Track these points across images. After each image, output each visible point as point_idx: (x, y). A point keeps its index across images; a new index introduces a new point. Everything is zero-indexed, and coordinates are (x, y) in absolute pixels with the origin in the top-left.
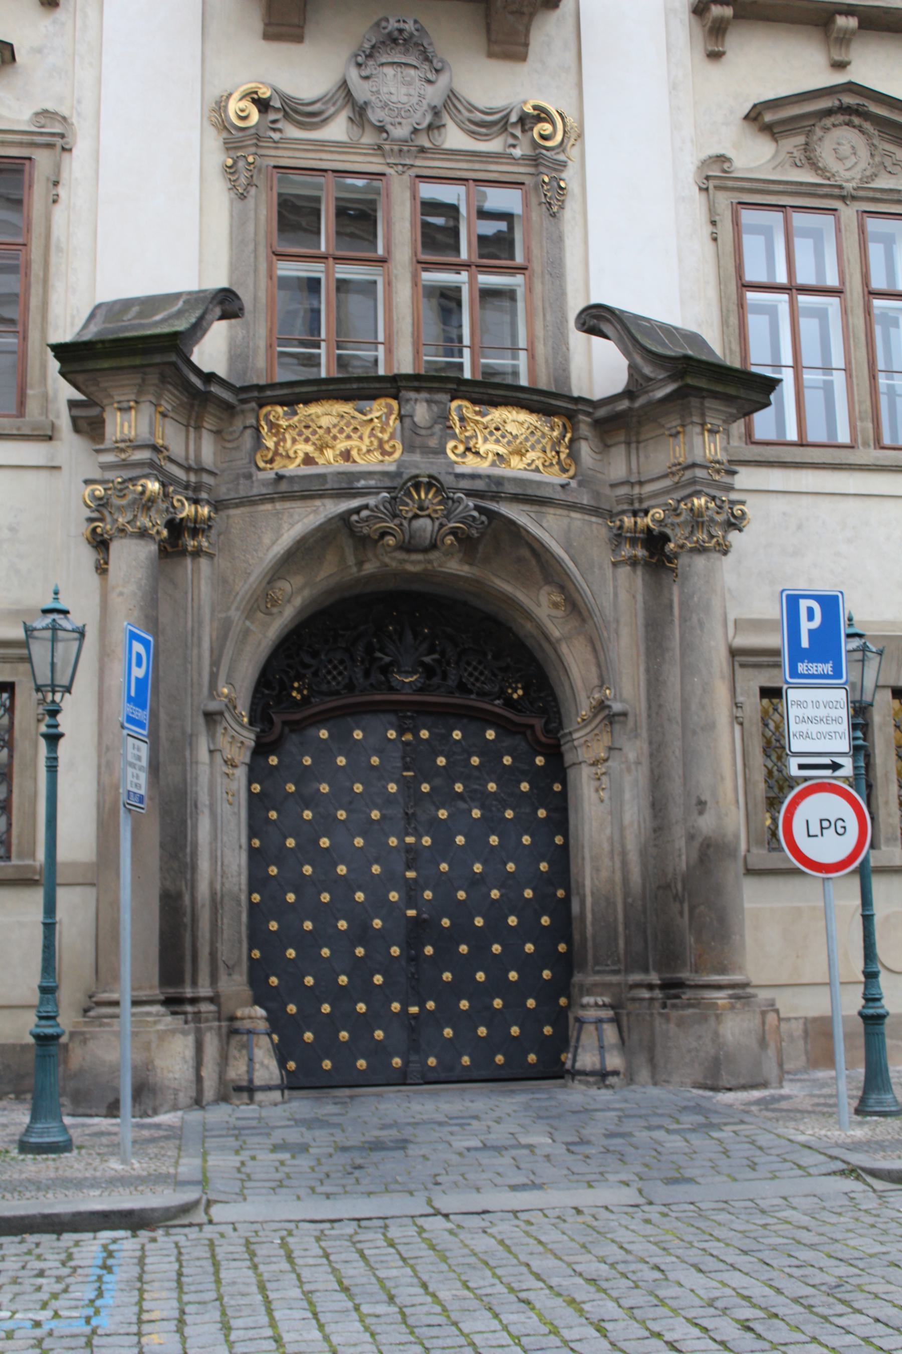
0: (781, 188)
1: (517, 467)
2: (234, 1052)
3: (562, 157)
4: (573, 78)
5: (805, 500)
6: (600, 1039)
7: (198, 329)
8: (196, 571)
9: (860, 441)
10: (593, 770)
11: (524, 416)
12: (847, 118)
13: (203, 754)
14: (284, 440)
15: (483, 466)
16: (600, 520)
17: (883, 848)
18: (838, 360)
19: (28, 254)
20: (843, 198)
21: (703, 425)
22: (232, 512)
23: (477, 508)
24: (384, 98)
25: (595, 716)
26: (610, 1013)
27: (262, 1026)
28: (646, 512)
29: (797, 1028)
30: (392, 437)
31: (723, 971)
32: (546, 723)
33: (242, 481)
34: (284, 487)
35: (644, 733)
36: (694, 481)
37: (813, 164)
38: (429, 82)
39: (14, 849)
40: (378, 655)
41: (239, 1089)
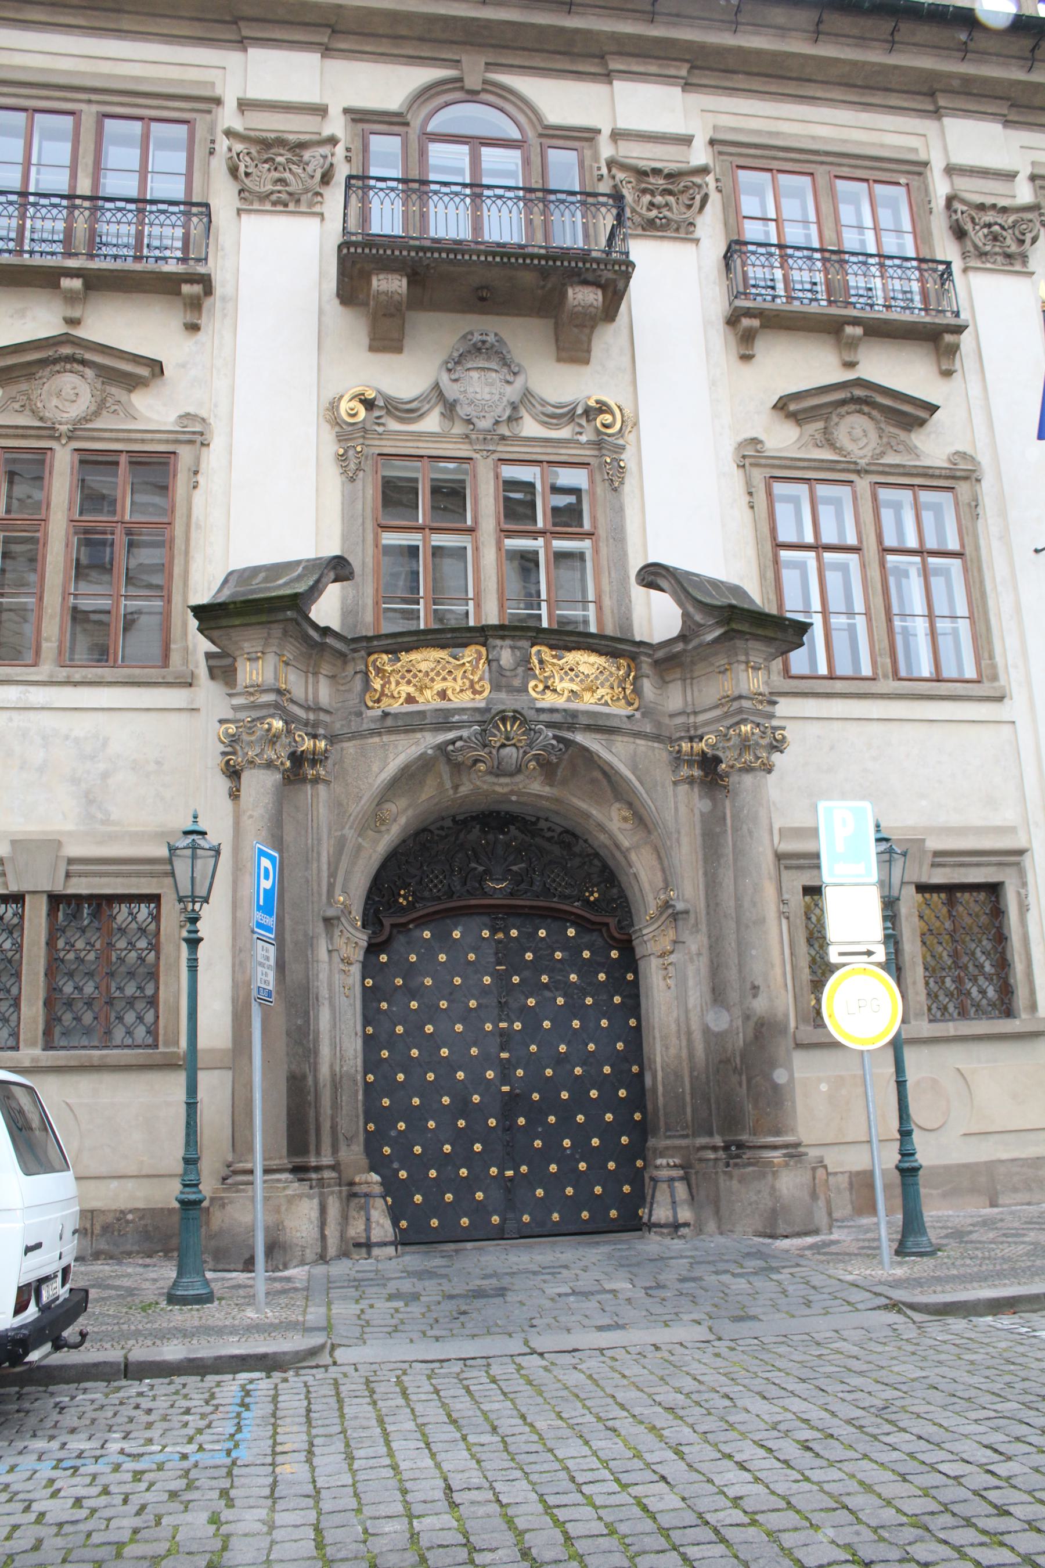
0: (805, 464)
1: (588, 702)
2: (353, 1213)
3: (621, 442)
4: (628, 377)
5: (836, 725)
6: (672, 1196)
7: (315, 591)
8: (315, 796)
9: (880, 672)
10: (661, 961)
11: (594, 658)
12: (858, 407)
13: (323, 954)
14: (389, 682)
15: (559, 702)
16: (661, 746)
17: (913, 1022)
18: (859, 606)
19: (172, 531)
20: (858, 472)
21: (747, 663)
22: (345, 745)
23: (555, 737)
24: (471, 396)
25: (661, 914)
26: (681, 1173)
27: (378, 1189)
28: (701, 739)
29: (843, 1181)
30: (480, 679)
31: (778, 1133)
32: (619, 922)
33: (353, 718)
34: (389, 722)
35: (704, 927)
36: (740, 711)
37: (831, 444)
38: (508, 382)
39: (161, 1038)
40: (473, 865)
41: (358, 1245)
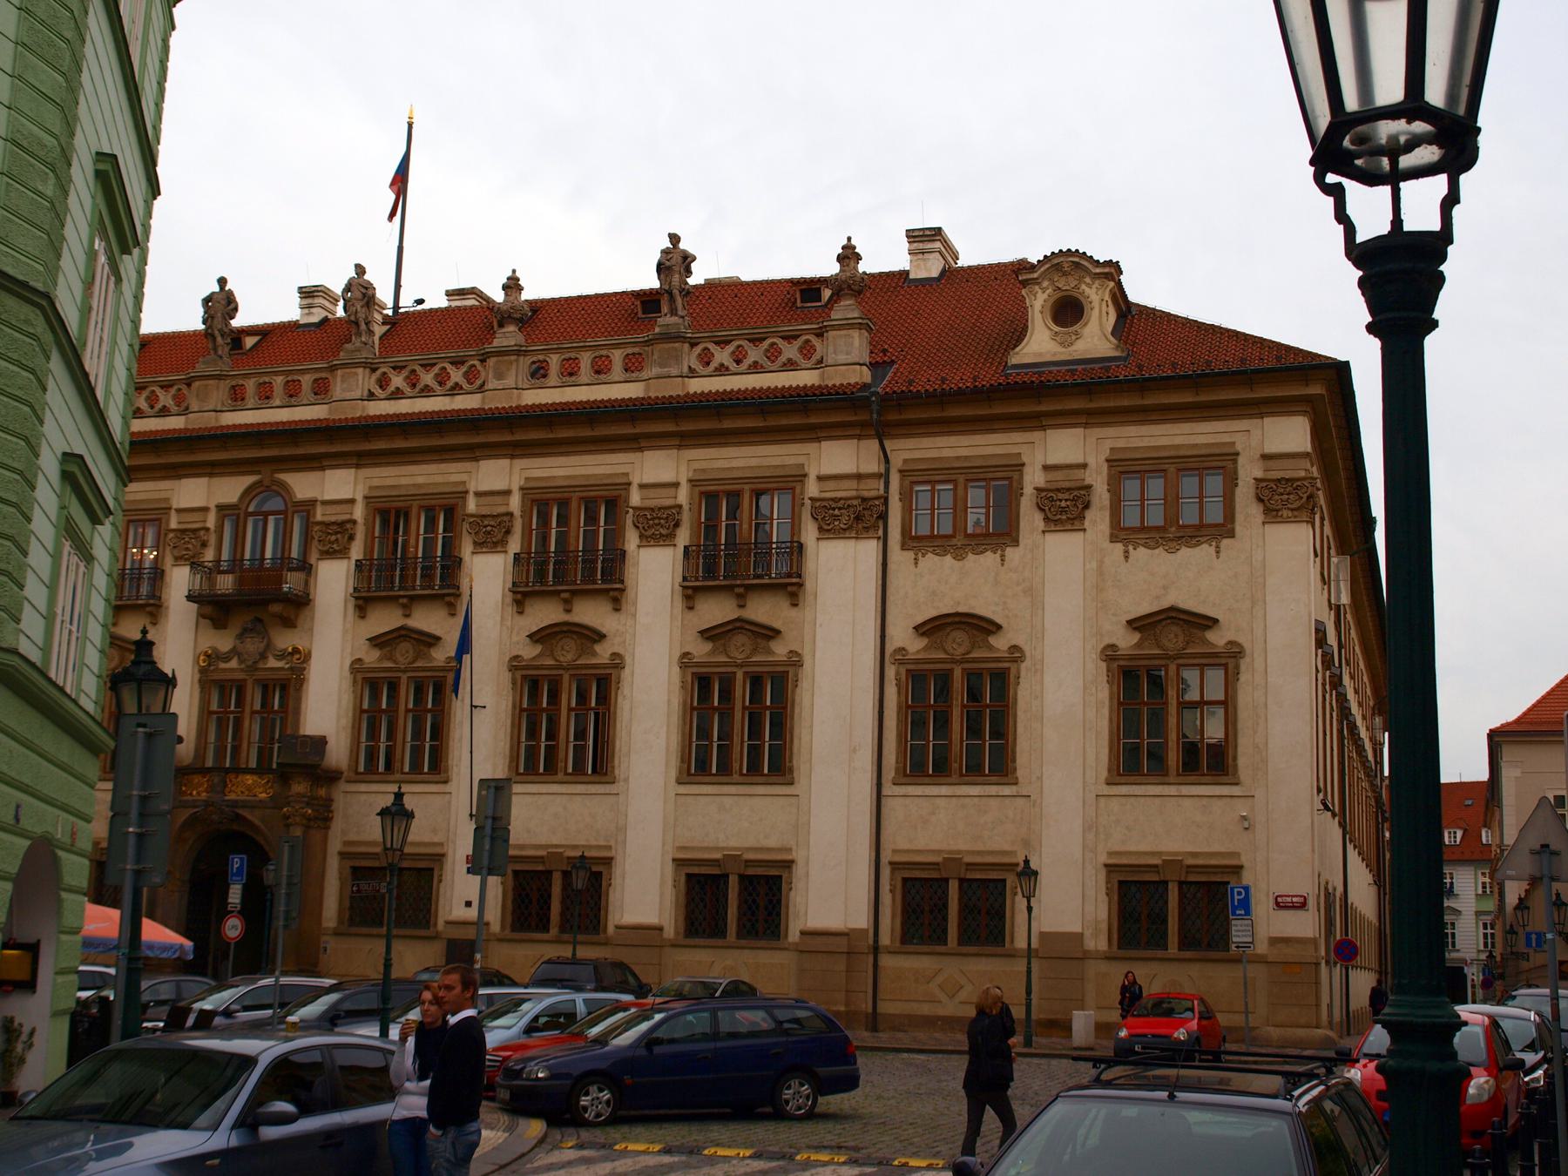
37: (391, 658)
